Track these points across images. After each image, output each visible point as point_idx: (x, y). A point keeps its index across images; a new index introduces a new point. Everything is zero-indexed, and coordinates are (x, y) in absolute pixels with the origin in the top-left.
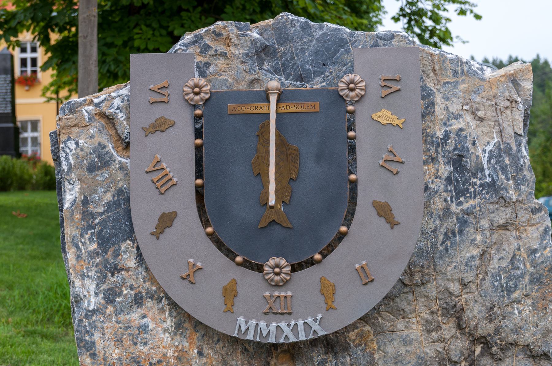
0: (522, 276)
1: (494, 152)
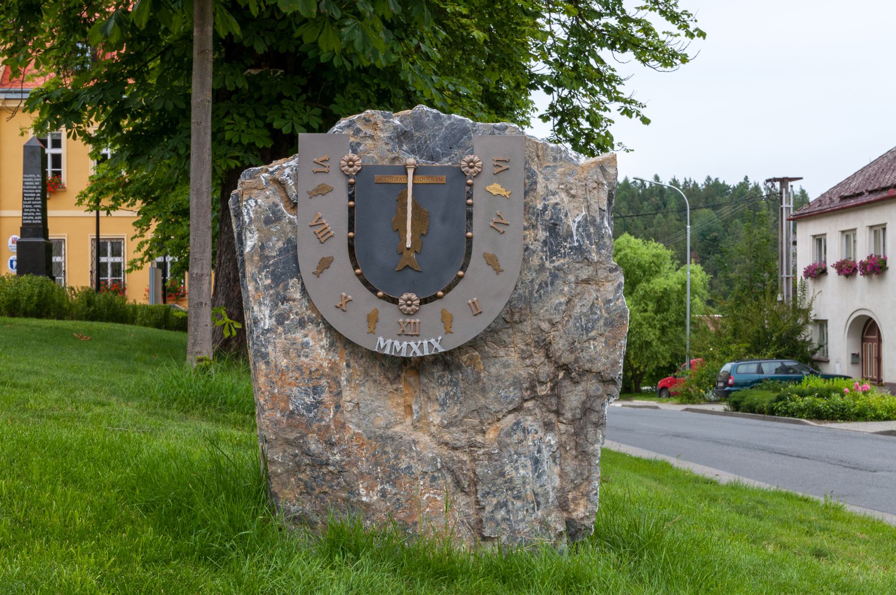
0: (598, 319)
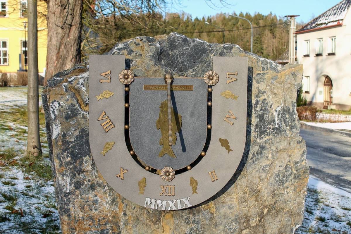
0: (290, 175)
1: (281, 112)
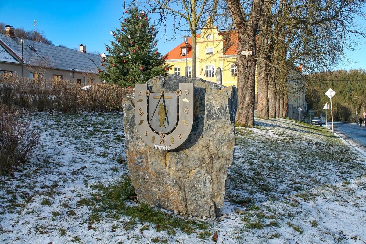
0: (225, 140)
